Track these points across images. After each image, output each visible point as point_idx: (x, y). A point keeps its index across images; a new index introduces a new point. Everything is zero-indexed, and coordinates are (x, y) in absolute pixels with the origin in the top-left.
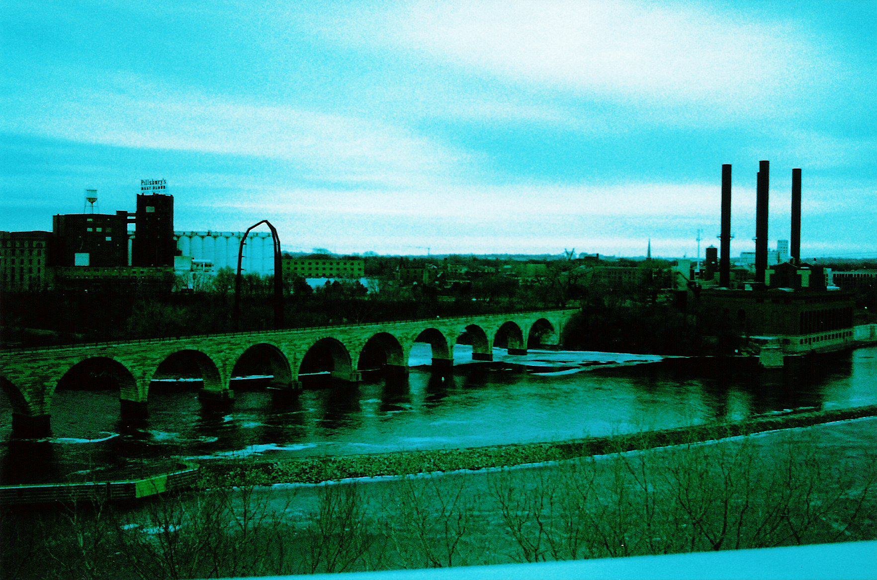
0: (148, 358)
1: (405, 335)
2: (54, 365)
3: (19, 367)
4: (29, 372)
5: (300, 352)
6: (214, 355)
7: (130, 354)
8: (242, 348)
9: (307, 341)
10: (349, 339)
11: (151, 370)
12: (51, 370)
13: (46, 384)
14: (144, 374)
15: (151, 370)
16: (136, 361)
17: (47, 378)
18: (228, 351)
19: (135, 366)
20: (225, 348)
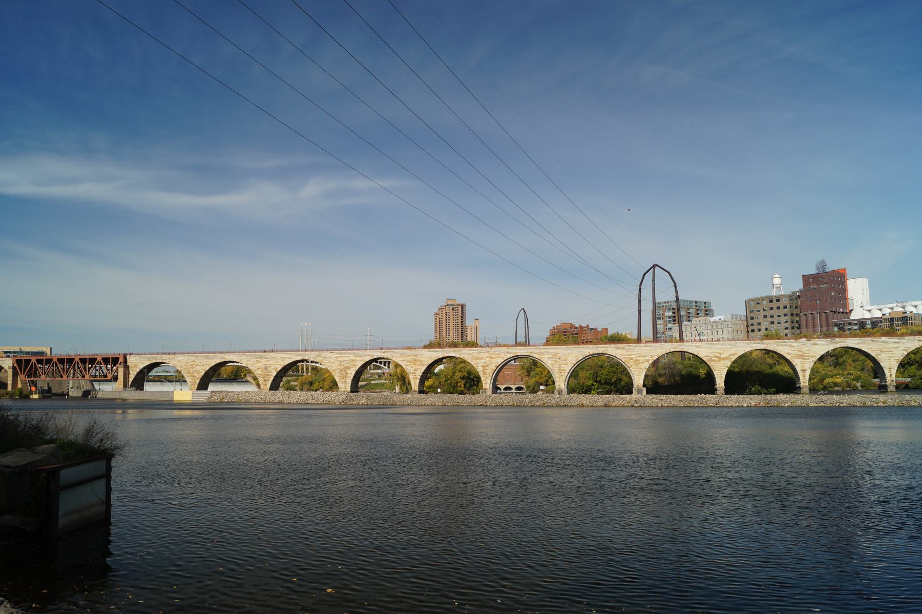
0: (419, 361)
1: (717, 354)
2: (353, 360)
3: (332, 360)
4: (339, 363)
5: (566, 364)
6: (476, 362)
7: (404, 357)
8: (502, 357)
9: (574, 355)
10: (629, 355)
11: (421, 369)
12: (351, 363)
13: (347, 371)
14: (416, 370)
15: (421, 369)
16: (409, 361)
17: (348, 368)
18: (487, 359)
19: (408, 365)
20: (486, 356)
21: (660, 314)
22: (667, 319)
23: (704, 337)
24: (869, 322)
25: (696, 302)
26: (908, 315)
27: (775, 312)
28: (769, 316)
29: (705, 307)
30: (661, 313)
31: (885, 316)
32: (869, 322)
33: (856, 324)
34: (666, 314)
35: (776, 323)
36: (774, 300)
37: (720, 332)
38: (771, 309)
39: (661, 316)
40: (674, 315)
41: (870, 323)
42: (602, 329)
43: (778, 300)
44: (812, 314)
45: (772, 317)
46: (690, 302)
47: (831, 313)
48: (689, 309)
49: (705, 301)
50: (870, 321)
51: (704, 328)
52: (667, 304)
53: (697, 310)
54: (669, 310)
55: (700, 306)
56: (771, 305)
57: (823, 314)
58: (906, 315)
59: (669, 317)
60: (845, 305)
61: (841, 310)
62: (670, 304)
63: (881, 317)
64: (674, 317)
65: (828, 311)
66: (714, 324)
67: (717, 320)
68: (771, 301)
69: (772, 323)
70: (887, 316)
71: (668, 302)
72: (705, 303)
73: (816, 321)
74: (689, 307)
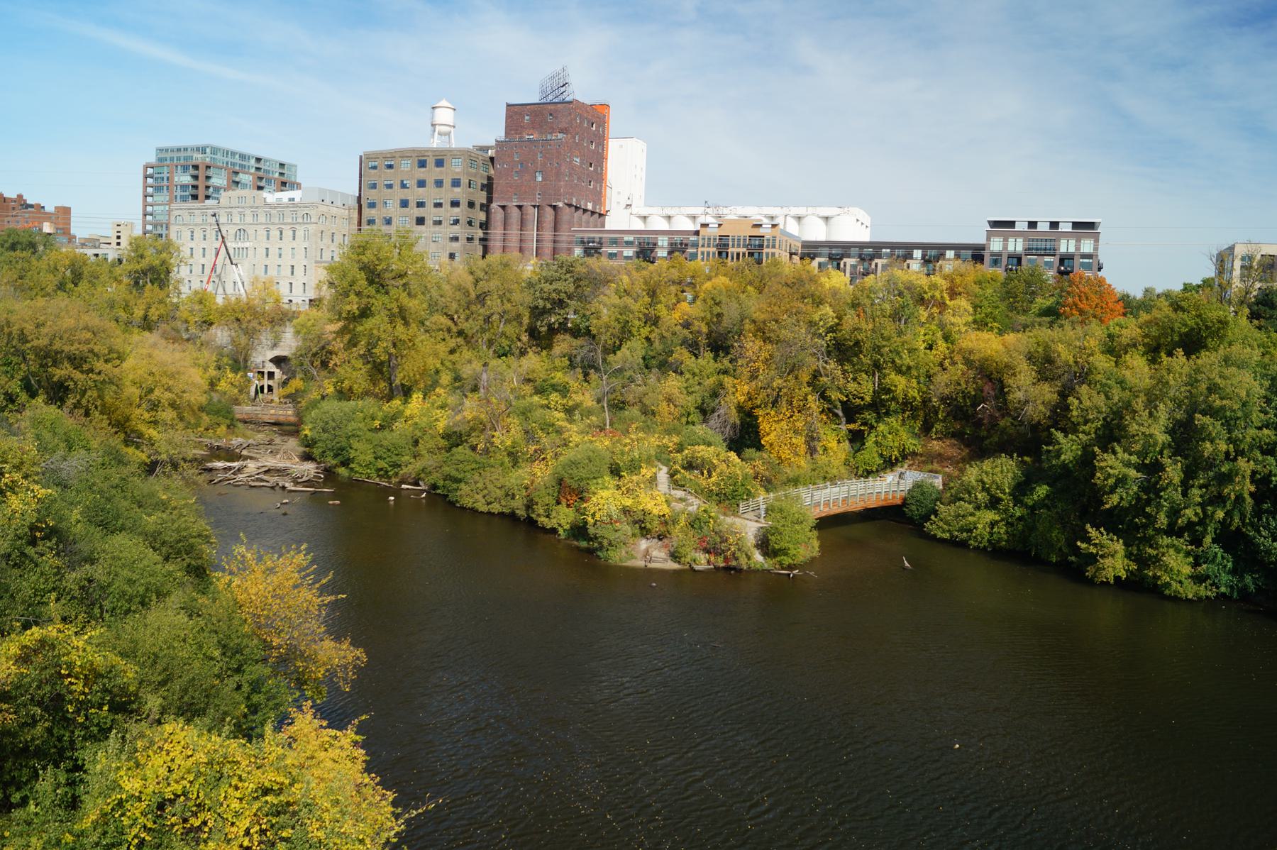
21: (163, 179)
22: (179, 193)
23: (247, 244)
24: (663, 241)
25: (258, 160)
26: (766, 231)
27: (430, 194)
28: (412, 204)
29: (281, 174)
30: (165, 175)
31: (708, 230)
32: (663, 241)
33: (629, 243)
34: (176, 179)
35: (429, 222)
36: (431, 162)
37: (288, 233)
38: (421, 184)
40: (194, 183)
41: (666, 244)
42: (56, 208)
43: (440, 163)
44: (520, 207)
45: (420, 205)
46: (243, 157)
47: (567, 209)
48: (236, 173)
49: (283, 161)
50: (666, 238)
51: (249, 219)
52: (182, 154)
53: (261, 179)
54: (185, 168)
55: (267, 171)
56: (421, 173)
57: (549, 211)
58: (760, 232)
59: (184, 187)
60: (598, 196)
61: (590, 207)
62: (189, 153)
63: (697, 233)
64: (195, 187)
65: (560, 204)
66: (274, 212)
67: (285, 200)
68: (422, 164)
69: (420, 221)
70: (713, 231)
71: (186, 149)
72: (282, 165)
73: (529, 227)
74: (237, 168)
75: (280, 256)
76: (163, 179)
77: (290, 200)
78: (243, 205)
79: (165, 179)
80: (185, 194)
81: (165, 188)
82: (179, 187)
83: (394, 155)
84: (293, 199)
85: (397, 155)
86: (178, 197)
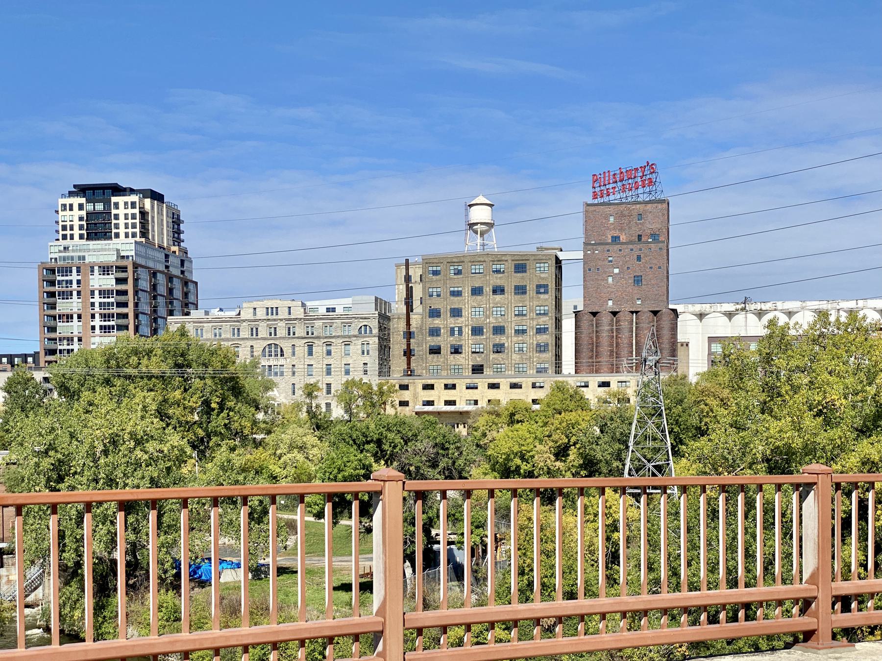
37: (319, 348)
39: (75, 285)
43: (520, 268)
54: (105, 270)
67: (322, 311)
75: (294, 373)
76: (71, 282)
77: (328, 310)
78: (274, 317)
79: (75, 282)
80: (106, 300)
81: (75, 293)
82: (97, 293)
83: (462, 259)
84: (334, 310)
85: (466, 260)
86: (97, 305)
